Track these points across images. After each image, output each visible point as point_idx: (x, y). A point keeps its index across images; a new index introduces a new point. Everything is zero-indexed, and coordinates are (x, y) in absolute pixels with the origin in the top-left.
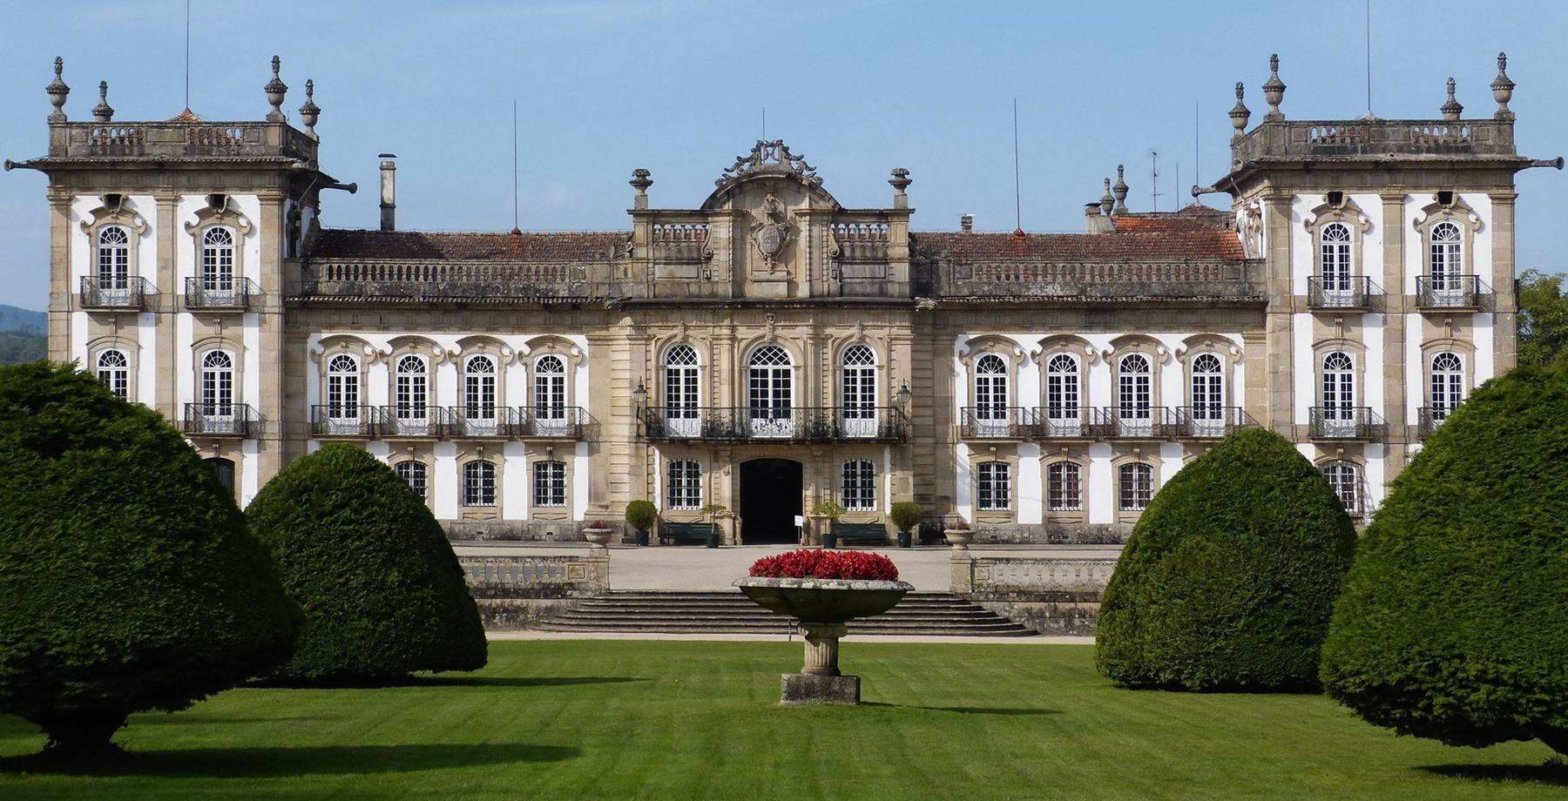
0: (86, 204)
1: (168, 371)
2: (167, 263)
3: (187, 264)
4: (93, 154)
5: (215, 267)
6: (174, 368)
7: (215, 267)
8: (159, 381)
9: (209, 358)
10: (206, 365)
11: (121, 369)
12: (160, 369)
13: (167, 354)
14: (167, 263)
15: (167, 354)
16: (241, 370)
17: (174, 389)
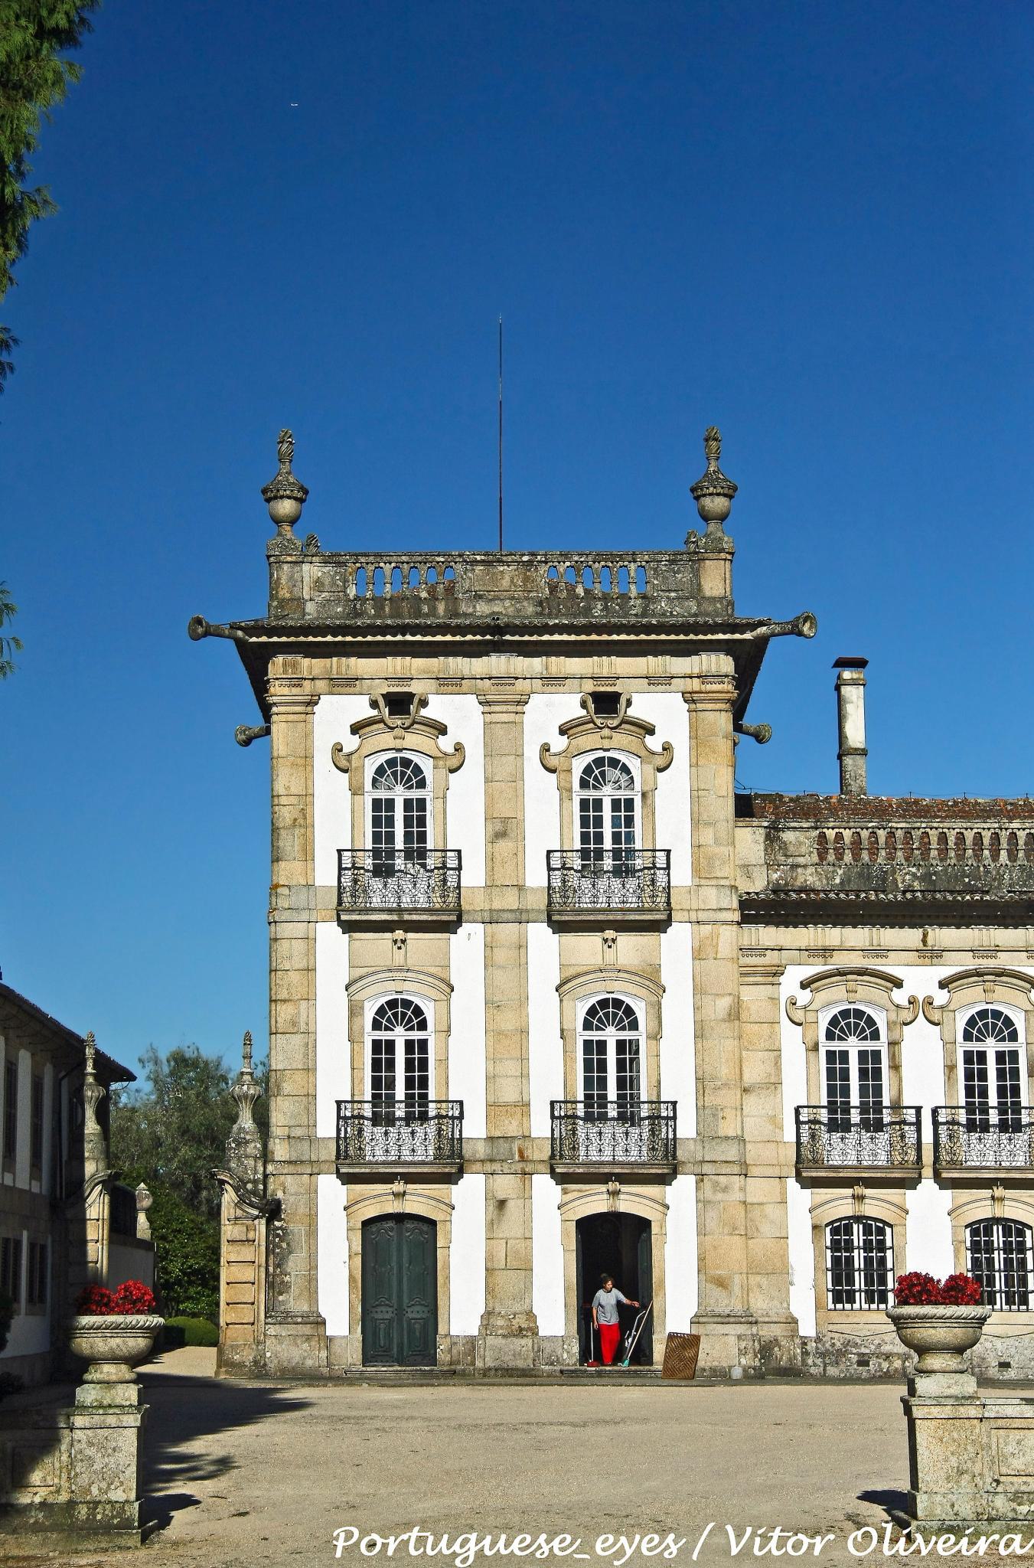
0: (337, 715)
1: (508, 1040)
2: (503, 829)
3: (548, 822)
4: (358, 614)
5: (606, 840)
6: (524, 1032)
7: (606, 840)
8: (493, 1058)
9: (592, 1012)
10: (587, 1026)
11: (416, 1035)
12: (494, 1033)
13: (505, 1007)
14: (503, 829)
15: (505, 1007)
16: (656, 1036)
17: (525, 1076)
